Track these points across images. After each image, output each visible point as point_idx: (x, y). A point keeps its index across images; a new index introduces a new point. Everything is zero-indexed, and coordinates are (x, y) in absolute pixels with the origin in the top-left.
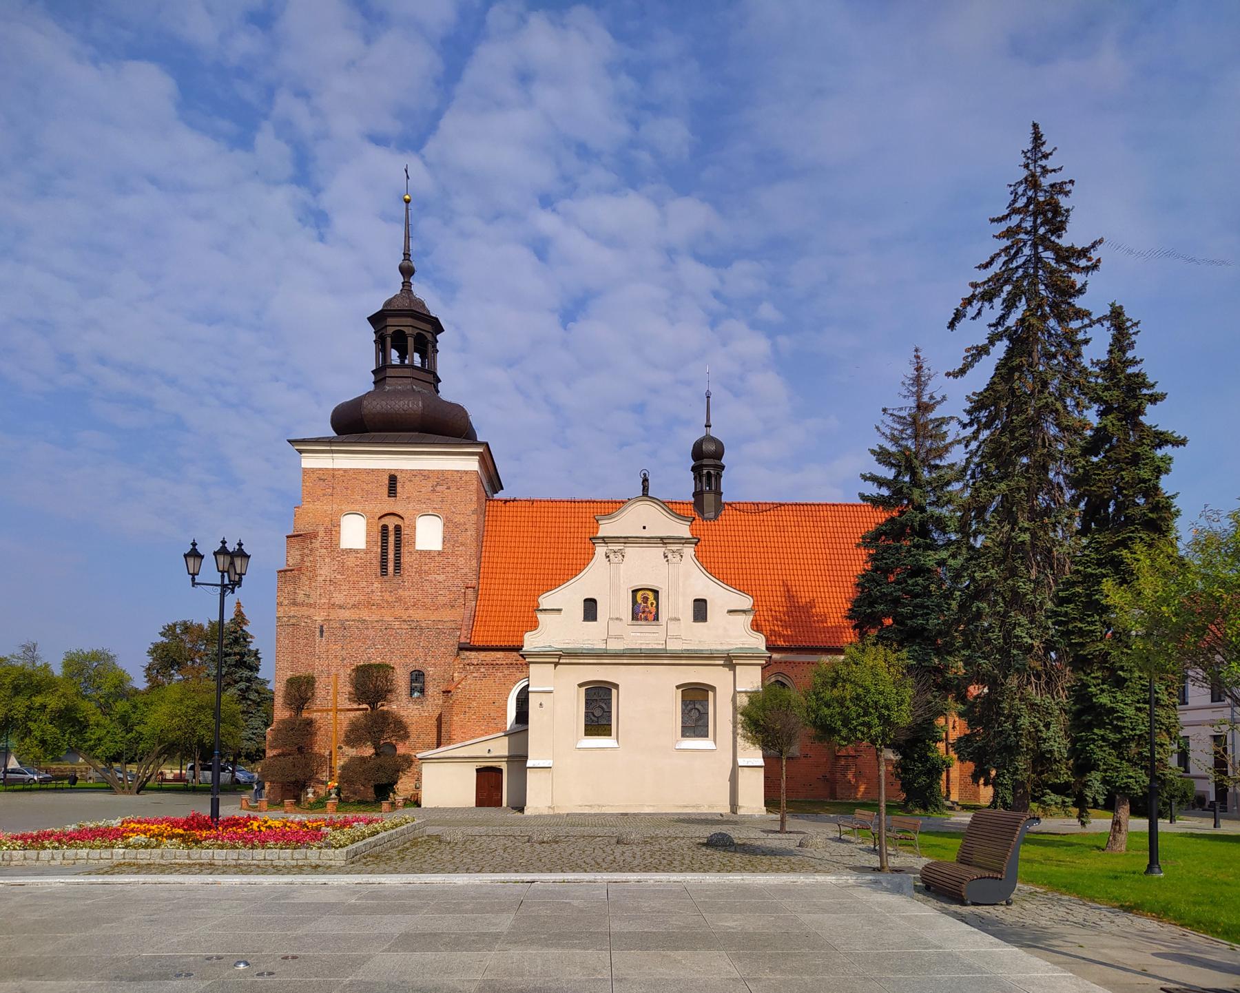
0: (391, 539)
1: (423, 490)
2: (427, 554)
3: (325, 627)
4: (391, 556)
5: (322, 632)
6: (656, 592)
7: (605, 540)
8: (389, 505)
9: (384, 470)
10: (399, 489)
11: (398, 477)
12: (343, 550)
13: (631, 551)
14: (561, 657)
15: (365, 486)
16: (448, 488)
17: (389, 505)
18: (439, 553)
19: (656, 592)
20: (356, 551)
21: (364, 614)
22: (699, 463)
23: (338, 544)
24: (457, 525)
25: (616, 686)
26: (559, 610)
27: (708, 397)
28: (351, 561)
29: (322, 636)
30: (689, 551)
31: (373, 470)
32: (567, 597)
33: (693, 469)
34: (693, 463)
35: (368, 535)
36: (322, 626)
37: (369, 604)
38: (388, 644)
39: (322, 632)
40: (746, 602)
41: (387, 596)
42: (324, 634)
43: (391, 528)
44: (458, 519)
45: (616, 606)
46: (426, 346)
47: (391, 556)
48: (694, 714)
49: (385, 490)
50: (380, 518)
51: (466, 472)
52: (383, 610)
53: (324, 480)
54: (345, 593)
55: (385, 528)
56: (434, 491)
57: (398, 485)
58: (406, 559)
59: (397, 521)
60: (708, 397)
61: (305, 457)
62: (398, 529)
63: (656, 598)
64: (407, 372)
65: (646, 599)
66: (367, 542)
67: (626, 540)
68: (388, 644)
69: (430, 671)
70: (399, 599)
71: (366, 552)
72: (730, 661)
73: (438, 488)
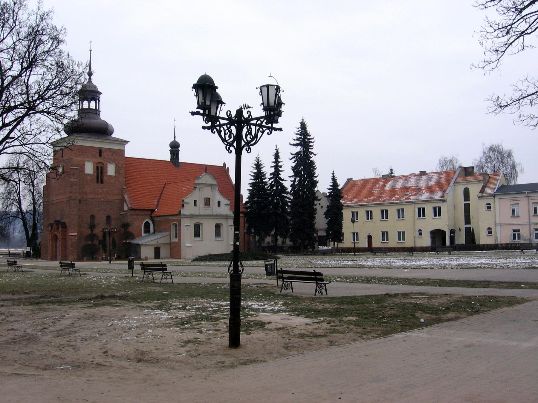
0: (100, 171)
6: (209, 199)
7: (199, 184)
8: (99, 160)
10: (102, 154)
11: (102, 150)
12: (86, 174)
13: (205, 188)
14: (192, 216)
17: (99, 160)
19: (209, 199)
24: (119, 167)
25: (202, 224)
26: (189, 203)
28: (89, 178)
29: (80, 203)
30: (217, 188)
32: (189, 200)
35: (93, 169)
36: (80, 200)
40: (228, 202)
41: (99, 190)
43: (99, 167)
44: (120, 165)
45: (201, 203)
48: (217, 231)
49: (98, 154)
50: (97, 164)
53: (80, 149)
55: (98, 167)
62: (101, 168)
63: (209, 200)
65: (207, 200)
71: (93, 175)
72: (227, 217)
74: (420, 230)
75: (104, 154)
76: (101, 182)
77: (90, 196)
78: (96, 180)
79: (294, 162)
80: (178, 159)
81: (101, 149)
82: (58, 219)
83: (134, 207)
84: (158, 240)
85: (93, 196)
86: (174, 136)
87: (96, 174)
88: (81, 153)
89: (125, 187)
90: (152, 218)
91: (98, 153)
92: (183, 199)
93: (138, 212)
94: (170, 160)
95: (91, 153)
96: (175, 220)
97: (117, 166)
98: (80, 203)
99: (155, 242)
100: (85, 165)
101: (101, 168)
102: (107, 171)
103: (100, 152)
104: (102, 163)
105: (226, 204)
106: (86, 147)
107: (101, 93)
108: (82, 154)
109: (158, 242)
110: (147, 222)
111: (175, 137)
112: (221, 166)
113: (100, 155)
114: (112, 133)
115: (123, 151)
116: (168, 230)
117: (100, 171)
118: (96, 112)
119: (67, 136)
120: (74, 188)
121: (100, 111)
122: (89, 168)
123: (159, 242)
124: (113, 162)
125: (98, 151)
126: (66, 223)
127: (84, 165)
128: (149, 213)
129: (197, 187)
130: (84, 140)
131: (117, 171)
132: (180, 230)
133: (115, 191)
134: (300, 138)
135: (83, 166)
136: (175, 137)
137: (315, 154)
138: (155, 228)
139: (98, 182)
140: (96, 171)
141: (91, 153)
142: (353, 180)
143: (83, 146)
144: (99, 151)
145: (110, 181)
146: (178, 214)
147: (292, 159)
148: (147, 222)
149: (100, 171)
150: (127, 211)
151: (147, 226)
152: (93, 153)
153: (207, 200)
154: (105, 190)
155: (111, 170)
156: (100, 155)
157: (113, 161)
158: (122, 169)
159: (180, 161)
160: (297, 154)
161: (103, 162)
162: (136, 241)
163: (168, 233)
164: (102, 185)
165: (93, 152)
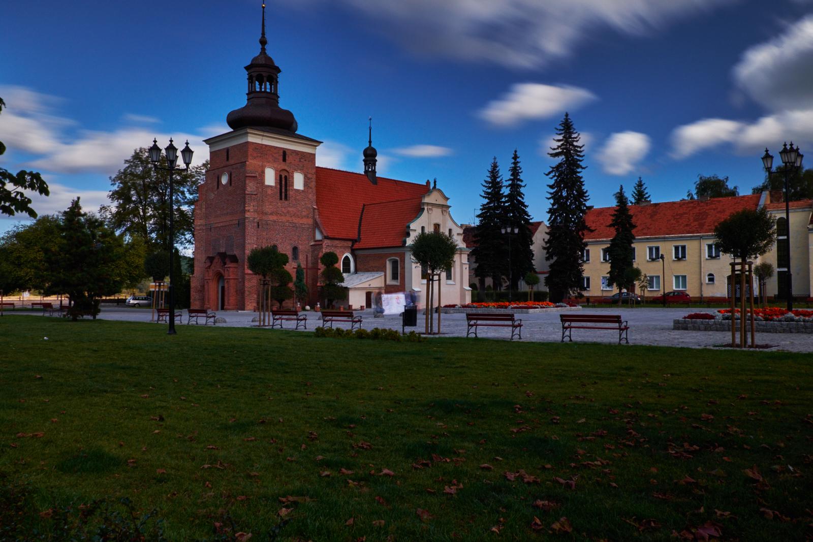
0: (283, 183)
1: (296, 160)
2: (298, 190)
3: (260, 223)
4: (283, 190)
5: (258, 226)
7: (428, 204)
8: (283, 166)
9: (281, 148)
10: (287, 158)
11: (287, 152)
13: (434, 209)
15: (273, 155)
16: (305, 160)
18: (303, 191)
20: (271, 186)
21: (275, 218)
22: (368, 158)
23: (264, 182)
24: (309, 179)
27: (370, 130)
29: (258, 227)
31: (277, 147)
33: (364, 160)
34: (364, 158)
35: (276, 179)
36: (258, 223)
37: (277, 214)
38: (284, 233)
39: (258, 226)
41: (283, 209)
42: (260, 227)
43: (283, 176)
44: (309, 176)
46: (273, 81)
47: (283, 190)
49: (281, 158)
50: (280, 171)
51: (311, 154)
52: (282, 217)
53: (257, 149)
54: (267, 207)
55: (281, 176)
56: (300, 161)
57: (287, 156)
58: (291, 193)
59: (286, 174)
60: (370, 130)
61: (250, 136)
62: (286, 177)
64: (264, 95)
66: (276, 183)
67: (433, 205)
68: (284, 233)
69: (300, 247)
70: (288, 212)
71: (276, 187)
73: (302, 160)
74: (710, 275)
75: (289, 159)
76: (286, 198)
77: (271, 218)
78: (278, 195)
79: (552, 178)
80: (374, 172)
81: (286, 151)
82: (222, 250)
83: (330, 235)
84: (368, 283)
85: (275, 218)
86: (369, 140)
87: (279, 186)
88: (259, 155)
89: (315, 207)
90: (353, 252)
91: (282, 156)
92: (408, 224)
93: (337, 242)
94: (363, 173)
95: (273, 156)
96: (395, 255)
97: (306, 177)
98: (258, 227)
99: (366, 285)
100: (264, 173)
101: (286, 177)
102: (293, 183)
103: (285, 153)
104: (285, 170)
105: (458, 234)
106: (266, 146)
107: (278, 70)
108: (260, 157)
109: (370, 285)
110: (347, 258)
111: (370, 142)
112: (424, 185)
113: (284, 160)
114: (296, 130)
115: (313, 156)
116: (383, 269)
117: (284, 181)
118: (273, 97)
119: (232, 130)
120: (252, 204)
121: (279, 97)
122: (270, 178)
123: (371, 286)
124: (300, 170)
125: (281, 152)
126: (237, 256)
127: (263, 172)
128: (350, 244)
129: (426, 208)
130: (263, 136)
131: (306, 184)
132: (403, 268)
133: (303, 213)
134: (562, 145)
135: (263, 173)
136: (370, 142)
137: (583, 166)
138: (358, 265)
139: (281, 199)
140: (279, 181)
141: (273, 156)
142: (595, 208)
143: (262, 145)
144: (282, 154)
145: (297, 197)
146: (401, 245)
147: (550, 173)
148: (347, 258)
149: (284, 181)
150: (321, 241)
151: (346, 261)
152: (275, 155)
153: (436, 227)
154: (290, 209)
155: (298, 182)
156: (284, 160)
157: (301, 169)
158: (312, 182)
159: (377, 176)
160: (560, 165)
161: (288, 170)
162: (344, 285)
163: (383, 274)
164: (287, 202)
165: (275, 154)
